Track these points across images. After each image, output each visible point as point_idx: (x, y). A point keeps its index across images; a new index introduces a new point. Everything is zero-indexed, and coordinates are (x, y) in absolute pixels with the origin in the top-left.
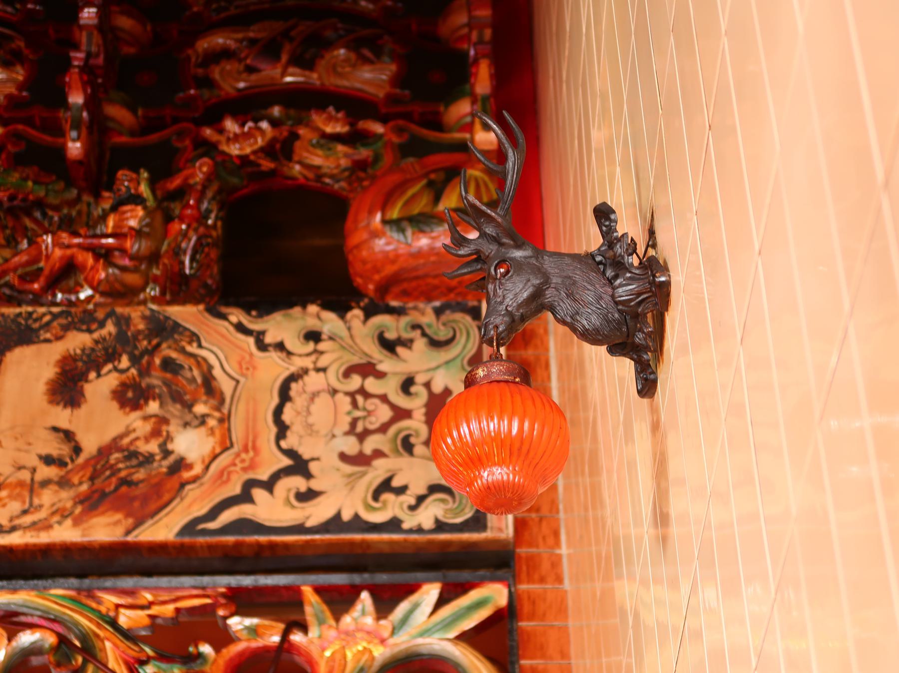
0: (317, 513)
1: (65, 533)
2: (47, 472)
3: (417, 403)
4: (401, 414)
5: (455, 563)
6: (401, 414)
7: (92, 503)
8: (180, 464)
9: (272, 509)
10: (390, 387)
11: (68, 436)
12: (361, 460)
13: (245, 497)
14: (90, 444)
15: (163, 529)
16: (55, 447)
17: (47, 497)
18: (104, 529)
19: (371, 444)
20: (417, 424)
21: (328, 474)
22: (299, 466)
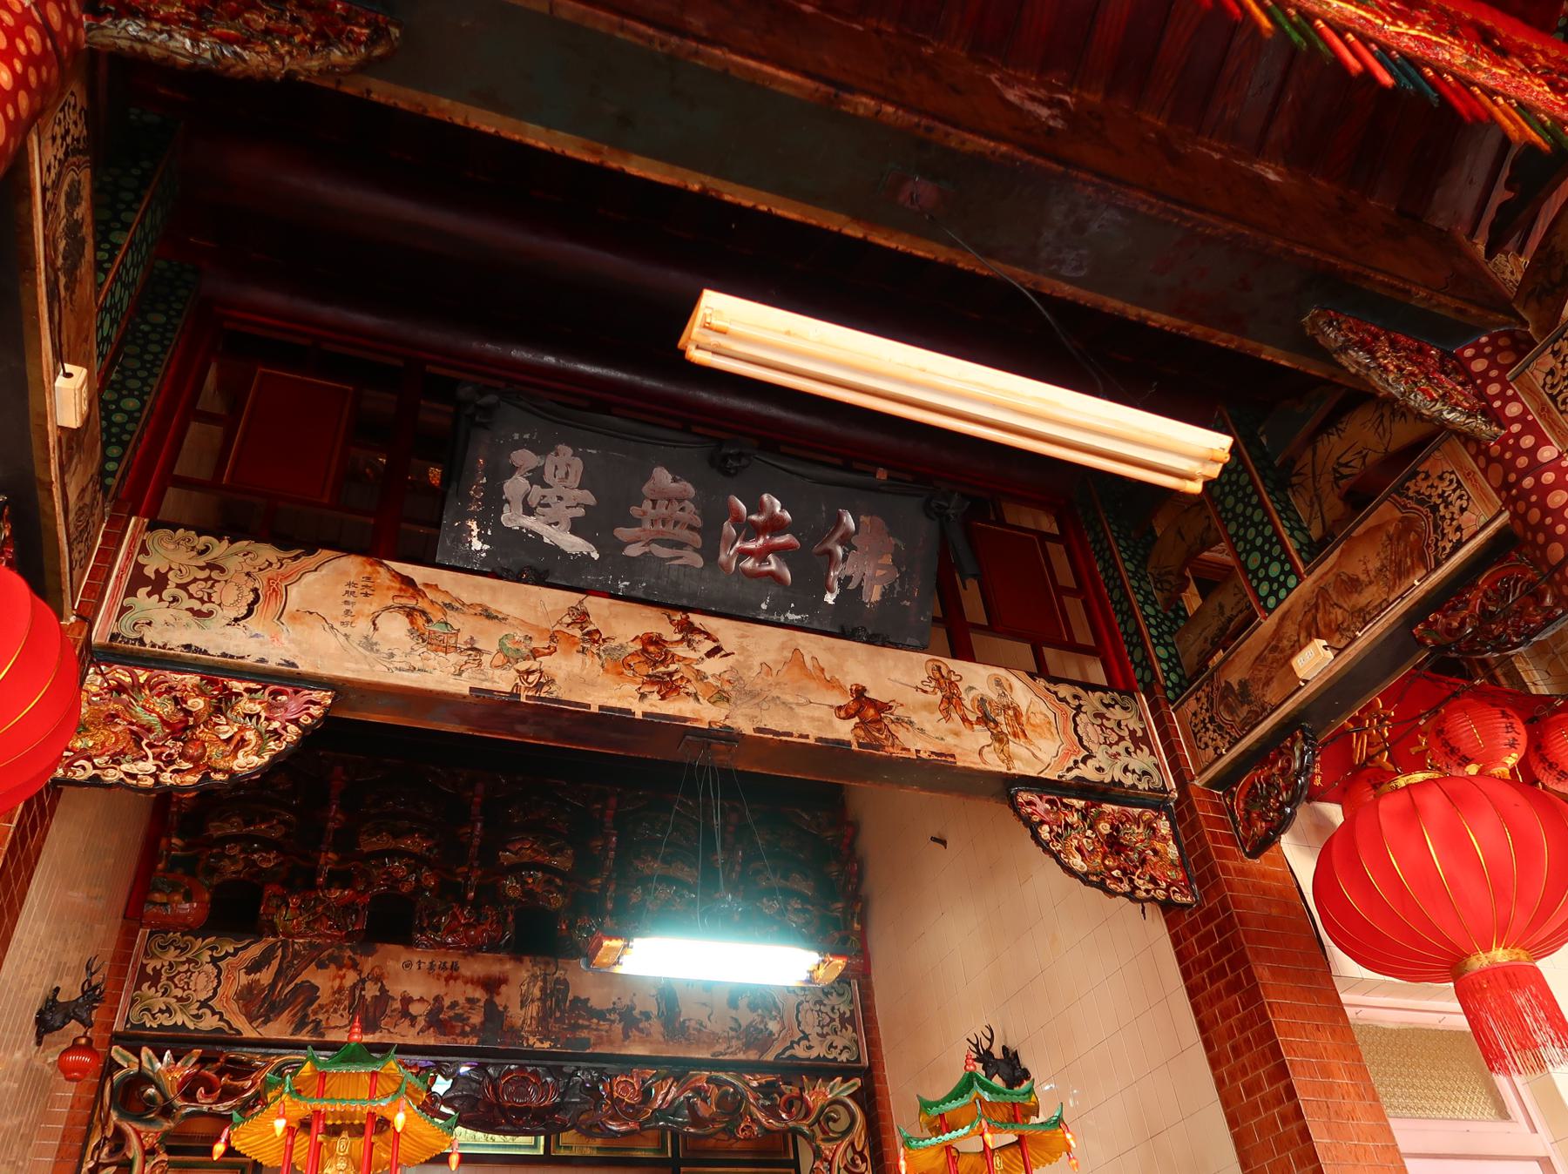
0: (813, 1054)
1: (741, 1056)
2: (732, 1033)
3: (836, 1016)
4: (833, 1020)
5: (846, 1072)
6: (833, 1020)
7: (748, 1046)
8: (771, 1034)
9: (800, 1051)
10: (827, 1009)
11: (736, 1020)
12: (823, 1036)
13: (791, 1047)
14: (744, 1023)
15: (770, 1057)
16: (733, 1025)
17: (734, 1043)
18: (753, 1056)
19: (826, 1030)
20: (837, 1023)
21: (814, 1040)
22: (806, 1037)
